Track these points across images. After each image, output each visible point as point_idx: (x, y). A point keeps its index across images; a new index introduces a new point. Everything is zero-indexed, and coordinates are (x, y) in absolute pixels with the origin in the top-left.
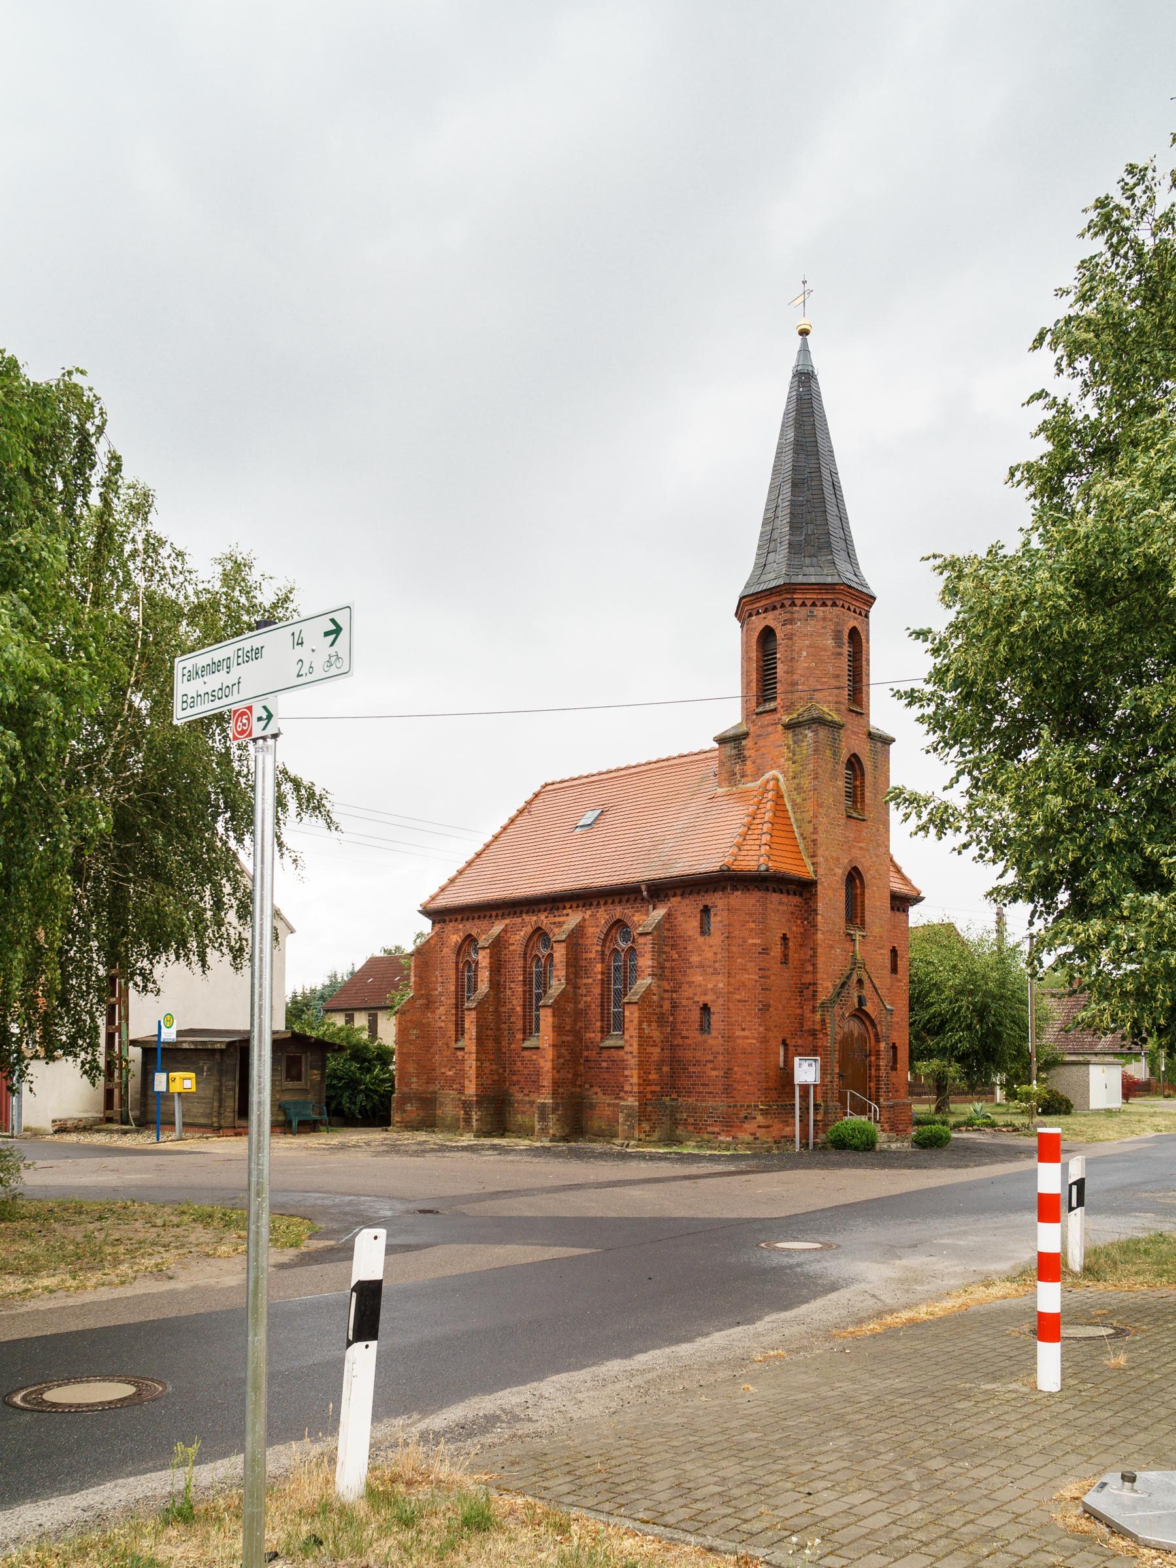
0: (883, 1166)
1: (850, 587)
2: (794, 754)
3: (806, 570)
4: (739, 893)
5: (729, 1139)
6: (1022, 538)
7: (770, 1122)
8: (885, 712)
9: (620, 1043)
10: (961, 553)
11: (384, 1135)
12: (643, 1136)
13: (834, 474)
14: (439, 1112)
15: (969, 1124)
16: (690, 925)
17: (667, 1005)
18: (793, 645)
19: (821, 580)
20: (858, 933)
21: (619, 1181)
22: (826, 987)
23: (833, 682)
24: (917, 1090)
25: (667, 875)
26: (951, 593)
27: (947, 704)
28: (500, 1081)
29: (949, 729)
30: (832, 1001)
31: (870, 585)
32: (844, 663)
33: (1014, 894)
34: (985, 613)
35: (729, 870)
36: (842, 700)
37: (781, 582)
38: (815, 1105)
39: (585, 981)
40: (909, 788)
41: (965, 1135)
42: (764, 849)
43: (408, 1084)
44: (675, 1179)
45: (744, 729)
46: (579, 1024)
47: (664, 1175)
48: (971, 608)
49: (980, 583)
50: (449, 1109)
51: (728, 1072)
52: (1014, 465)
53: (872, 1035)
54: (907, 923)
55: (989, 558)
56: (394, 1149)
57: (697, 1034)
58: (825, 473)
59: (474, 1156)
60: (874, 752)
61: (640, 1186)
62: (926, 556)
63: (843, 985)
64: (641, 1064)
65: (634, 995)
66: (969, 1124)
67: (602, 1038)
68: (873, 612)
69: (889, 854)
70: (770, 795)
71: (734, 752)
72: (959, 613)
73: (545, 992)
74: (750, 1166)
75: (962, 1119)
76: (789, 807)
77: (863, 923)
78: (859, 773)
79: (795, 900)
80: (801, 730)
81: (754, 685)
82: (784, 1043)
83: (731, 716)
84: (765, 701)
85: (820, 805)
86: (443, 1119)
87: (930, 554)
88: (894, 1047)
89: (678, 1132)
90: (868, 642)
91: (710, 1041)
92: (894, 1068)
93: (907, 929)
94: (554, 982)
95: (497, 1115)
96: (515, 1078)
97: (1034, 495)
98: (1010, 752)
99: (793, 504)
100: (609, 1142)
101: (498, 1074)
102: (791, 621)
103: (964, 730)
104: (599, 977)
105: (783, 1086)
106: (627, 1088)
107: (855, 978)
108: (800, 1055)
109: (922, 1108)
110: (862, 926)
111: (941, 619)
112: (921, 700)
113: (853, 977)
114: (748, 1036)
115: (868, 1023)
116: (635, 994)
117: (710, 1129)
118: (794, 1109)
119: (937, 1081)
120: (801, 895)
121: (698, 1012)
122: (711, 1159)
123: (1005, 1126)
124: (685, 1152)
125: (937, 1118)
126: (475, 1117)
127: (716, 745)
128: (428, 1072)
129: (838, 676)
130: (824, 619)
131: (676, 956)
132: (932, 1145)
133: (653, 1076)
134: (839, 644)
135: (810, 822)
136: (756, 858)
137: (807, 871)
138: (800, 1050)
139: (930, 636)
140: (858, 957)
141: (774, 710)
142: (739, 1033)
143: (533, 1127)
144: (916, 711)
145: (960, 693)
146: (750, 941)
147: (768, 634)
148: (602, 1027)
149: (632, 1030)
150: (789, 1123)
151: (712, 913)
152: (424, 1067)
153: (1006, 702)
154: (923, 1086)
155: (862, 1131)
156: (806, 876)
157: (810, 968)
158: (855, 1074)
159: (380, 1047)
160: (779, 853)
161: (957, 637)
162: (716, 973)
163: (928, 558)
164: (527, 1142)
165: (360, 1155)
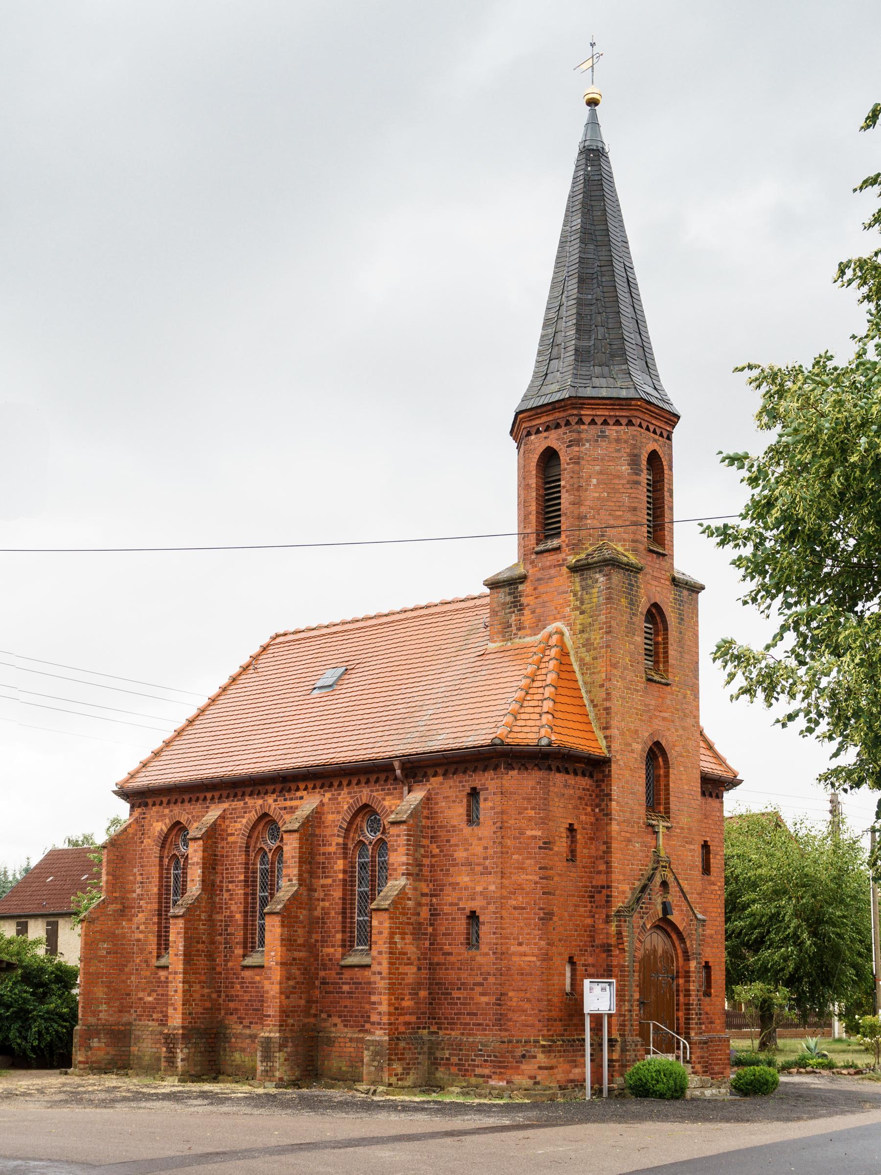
0: (695, 1119)
1: (649, 403)
2: (582, 603)
3: (596, 382)
4: (515, 772)
5: (503, 1084)
6: (856, 347)
7: (553, 1062)
8: (690, 552)
9: (366, 960)
10: (782, 362)
11: (63, 1079)
12: (393, 1080)
13: (628, 268)
14: (134, 1049)
15: (801, 1064)
16: (454, 812)
17: (425, 912)
18: (581, 470)
19: (614, 394)
20: (662, 824)
21: (363, 1139)
22: (623, 891)
23: (629, 516)
24: (736, 1021)
25: (427, 749)
26: (770, 415)
27: (768, 544)
28: (214, 1009)
29: (772, 575)
30: (630, 909)
31: (672, 401)
32: (642, 494)
33: (854, 778)
34: (812, 439)
35: (502, 744)
36: (639, 537)
37: (565, 394)
38: (610, 1040)
39: (323, 881)
40: (739, 642)
41: (796, 1079)
42: (546, 718)
43: (95, 1013)
44: (434, 1135)
45: (521, 571)
46: (314, 936)
47: (420, 1130)
48: (796, 430)
49: (807, 402)
50: (147, 1046)
51: (501, 999)
52: (845, 261)
53: (679, 951)
54: (722, 811)
55: (816, 371)
56: (75, 1098)
57: (462, 949)
58: (618, 267)
59: (178, 1107)
60: (679, 601)
61: (390, 1146)
62: (740, 366)
63: (644, 889)
64: (392, 989)
65: (383, 900)
66: (801, 1064)
67: (343, 955)
68: (678, 433)
69: (699, 726)
70: (553, 652)
71: (509, 599)
72: (781, 436)
73: (272, 895)
74: (529, 1119)
75: (792, 1058)
76: (576, 667)
77: (667, 811)
78: (660, 626)
79: (585, 782)
80: (590, 573)
81: (533, 518)
82: (571, 961)
83: (505, 556)
84: (547, 537)
85: (614, 666)
86: (139, 1058)
87: (745, 364)
88: (707, 967)
89: (439, 1075)
90: (671, 469)
91: (479, 959)
92: (707, 994)
93: (722, 819)
94: (284, 883)
95: (209, 1054)
96: (232, 1005)
97: (868, 298)
98: (847, 599)
99: (580, 303)
100: (350, 1088)
101: (211, 1000)
102: (577, 442)
103: (789, 576)
104: (341, 876)
105: (571, 1016)
106: (374, 1018)
107: (658, 880)
108: (591, 976)
109: (743, 1044)
110: (667, 815)
111: (759, 442)
112: (736, 538)
113: (656, 879)
114: (526, 952)
115: (674, 937)
116: (385, 898)
117: (478, 1071)
118: (583, 1045)
119: (761, 1008)
120: (591, 776)
121: (464, 921)
122: (480, 1109)
123: (845, 1067)
124: (447, 1100)
125: (762, 1056)
126: (180, 1056)
127: (487, 591)
128: (121, 998)
129: (635, 509)
130: (618, 440)
131: (436, 851)
132: (755, 1091)
133: (407, 1003)
134: (637, 472)
135: (602, 686)
136: (536, 729)
137: (598, 746)
138: (591, 970)
139: (746, 462)
140: (662, 854)
141: (558, 549)
142: (514, 948)
143: (254, 1070)
144: (730, 552)
145: (784, 531)
146: (529, 833)
147: (549, 457)
148: (343, 940)
149: (381, 944)
150: (577, 1063)
151: (482, 798)
152: (116, 990)
153: (838, 543)
154: (743, 1016)
155: (669, 1074)
156: (597, 752)
157: (603, 867)
158: (659, 1003)
159: (59, 967)
160: (566, 724)
161: (778, 464)
162: (486, 872)
163: (743, 369)
164: (246, 1088)
165: (31, 1105)
